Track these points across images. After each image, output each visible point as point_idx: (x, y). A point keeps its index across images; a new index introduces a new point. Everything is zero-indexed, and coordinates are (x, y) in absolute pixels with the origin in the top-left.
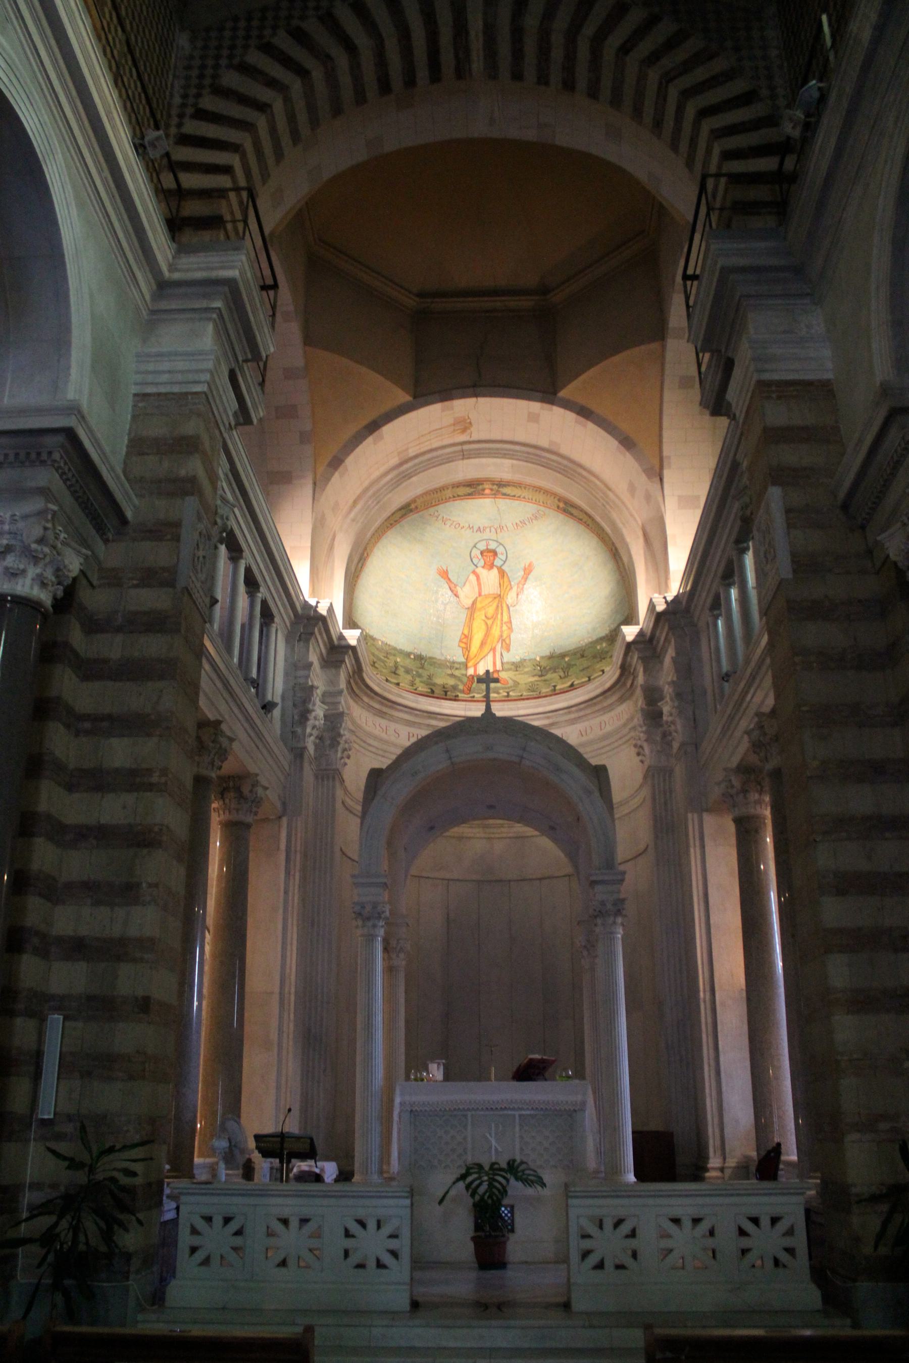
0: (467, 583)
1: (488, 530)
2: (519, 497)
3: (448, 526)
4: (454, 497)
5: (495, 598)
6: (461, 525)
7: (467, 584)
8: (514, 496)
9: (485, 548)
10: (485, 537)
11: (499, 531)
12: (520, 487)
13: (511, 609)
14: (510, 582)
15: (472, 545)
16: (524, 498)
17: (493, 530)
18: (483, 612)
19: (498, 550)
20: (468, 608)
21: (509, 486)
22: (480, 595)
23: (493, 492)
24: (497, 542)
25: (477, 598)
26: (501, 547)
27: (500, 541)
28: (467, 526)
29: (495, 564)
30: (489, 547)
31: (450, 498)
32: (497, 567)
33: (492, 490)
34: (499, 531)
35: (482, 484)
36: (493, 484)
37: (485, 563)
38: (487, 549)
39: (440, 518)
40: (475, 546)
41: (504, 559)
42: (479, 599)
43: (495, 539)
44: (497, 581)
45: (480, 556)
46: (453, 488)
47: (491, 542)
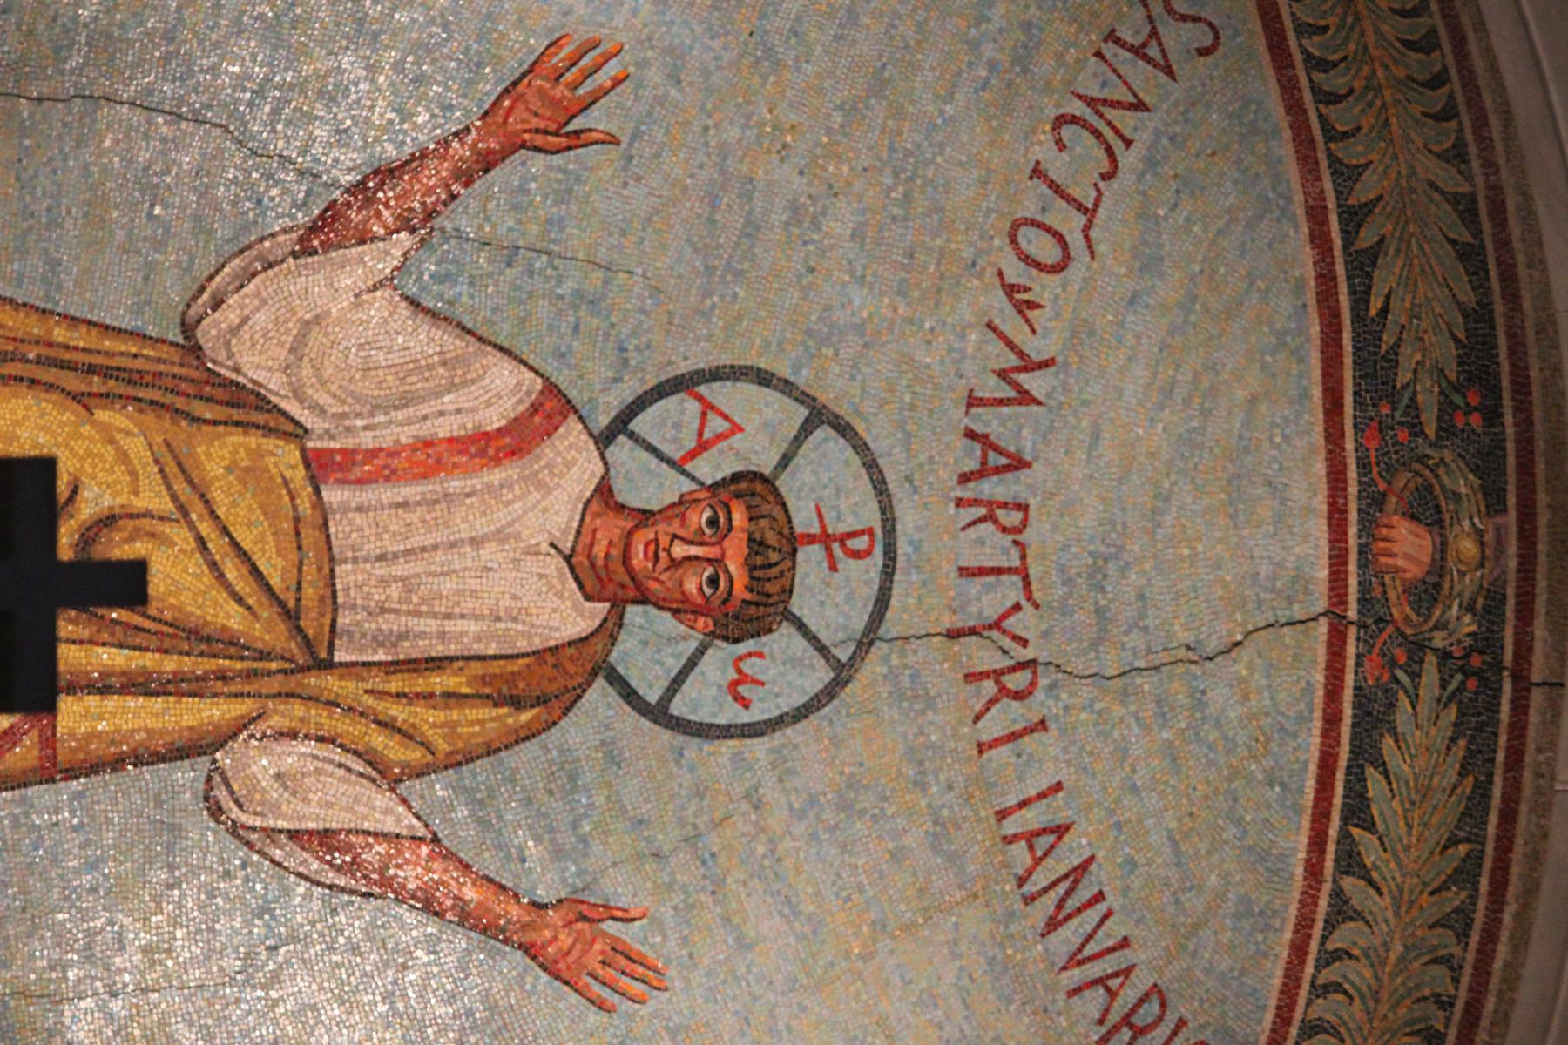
0: (453, 343)
1: (992, 547)
2: (1350, 862)
3: (1043, 150)
4: (1354, 218)
5: (292, 616)
6: (1044, 288)
7: (426, 340)
8: (1358, 811)
9: (803, 519)
10: (908, 520)
11: (983, 655)
12: (1464, 875)
13: (187, 775)
14: (458, 760)
15: (834, 390)
16: (1342, 910)
17: (991, 599)
18: (153, 498)
19: (784, 639)
20: (196, 350)
21: (1476, 761)
22: (319, 466)
23: (1400, 610)
24: (867, 640)
25: (296, 432)
26: (822, 675)
27: (872, 668)
28: (1036, 348)
29: (634, 613)
30: (810, 559)
31: (1347, 175)
32: (610, 630)
33: (1428, 592)
34: (983, 655)
35: (1494, 502)
36: (1488, 607)
37: (645, 516)
38: (793, 542)
39: (1139, 74)
40: (818, 416)
41: (677, 707)
42: (285, 458)
43: (893, 624)
44: (468, 634)
45: (709, 469)
46: (1466, 208)
47: (862, 575)
